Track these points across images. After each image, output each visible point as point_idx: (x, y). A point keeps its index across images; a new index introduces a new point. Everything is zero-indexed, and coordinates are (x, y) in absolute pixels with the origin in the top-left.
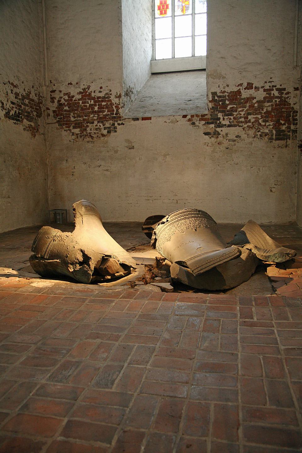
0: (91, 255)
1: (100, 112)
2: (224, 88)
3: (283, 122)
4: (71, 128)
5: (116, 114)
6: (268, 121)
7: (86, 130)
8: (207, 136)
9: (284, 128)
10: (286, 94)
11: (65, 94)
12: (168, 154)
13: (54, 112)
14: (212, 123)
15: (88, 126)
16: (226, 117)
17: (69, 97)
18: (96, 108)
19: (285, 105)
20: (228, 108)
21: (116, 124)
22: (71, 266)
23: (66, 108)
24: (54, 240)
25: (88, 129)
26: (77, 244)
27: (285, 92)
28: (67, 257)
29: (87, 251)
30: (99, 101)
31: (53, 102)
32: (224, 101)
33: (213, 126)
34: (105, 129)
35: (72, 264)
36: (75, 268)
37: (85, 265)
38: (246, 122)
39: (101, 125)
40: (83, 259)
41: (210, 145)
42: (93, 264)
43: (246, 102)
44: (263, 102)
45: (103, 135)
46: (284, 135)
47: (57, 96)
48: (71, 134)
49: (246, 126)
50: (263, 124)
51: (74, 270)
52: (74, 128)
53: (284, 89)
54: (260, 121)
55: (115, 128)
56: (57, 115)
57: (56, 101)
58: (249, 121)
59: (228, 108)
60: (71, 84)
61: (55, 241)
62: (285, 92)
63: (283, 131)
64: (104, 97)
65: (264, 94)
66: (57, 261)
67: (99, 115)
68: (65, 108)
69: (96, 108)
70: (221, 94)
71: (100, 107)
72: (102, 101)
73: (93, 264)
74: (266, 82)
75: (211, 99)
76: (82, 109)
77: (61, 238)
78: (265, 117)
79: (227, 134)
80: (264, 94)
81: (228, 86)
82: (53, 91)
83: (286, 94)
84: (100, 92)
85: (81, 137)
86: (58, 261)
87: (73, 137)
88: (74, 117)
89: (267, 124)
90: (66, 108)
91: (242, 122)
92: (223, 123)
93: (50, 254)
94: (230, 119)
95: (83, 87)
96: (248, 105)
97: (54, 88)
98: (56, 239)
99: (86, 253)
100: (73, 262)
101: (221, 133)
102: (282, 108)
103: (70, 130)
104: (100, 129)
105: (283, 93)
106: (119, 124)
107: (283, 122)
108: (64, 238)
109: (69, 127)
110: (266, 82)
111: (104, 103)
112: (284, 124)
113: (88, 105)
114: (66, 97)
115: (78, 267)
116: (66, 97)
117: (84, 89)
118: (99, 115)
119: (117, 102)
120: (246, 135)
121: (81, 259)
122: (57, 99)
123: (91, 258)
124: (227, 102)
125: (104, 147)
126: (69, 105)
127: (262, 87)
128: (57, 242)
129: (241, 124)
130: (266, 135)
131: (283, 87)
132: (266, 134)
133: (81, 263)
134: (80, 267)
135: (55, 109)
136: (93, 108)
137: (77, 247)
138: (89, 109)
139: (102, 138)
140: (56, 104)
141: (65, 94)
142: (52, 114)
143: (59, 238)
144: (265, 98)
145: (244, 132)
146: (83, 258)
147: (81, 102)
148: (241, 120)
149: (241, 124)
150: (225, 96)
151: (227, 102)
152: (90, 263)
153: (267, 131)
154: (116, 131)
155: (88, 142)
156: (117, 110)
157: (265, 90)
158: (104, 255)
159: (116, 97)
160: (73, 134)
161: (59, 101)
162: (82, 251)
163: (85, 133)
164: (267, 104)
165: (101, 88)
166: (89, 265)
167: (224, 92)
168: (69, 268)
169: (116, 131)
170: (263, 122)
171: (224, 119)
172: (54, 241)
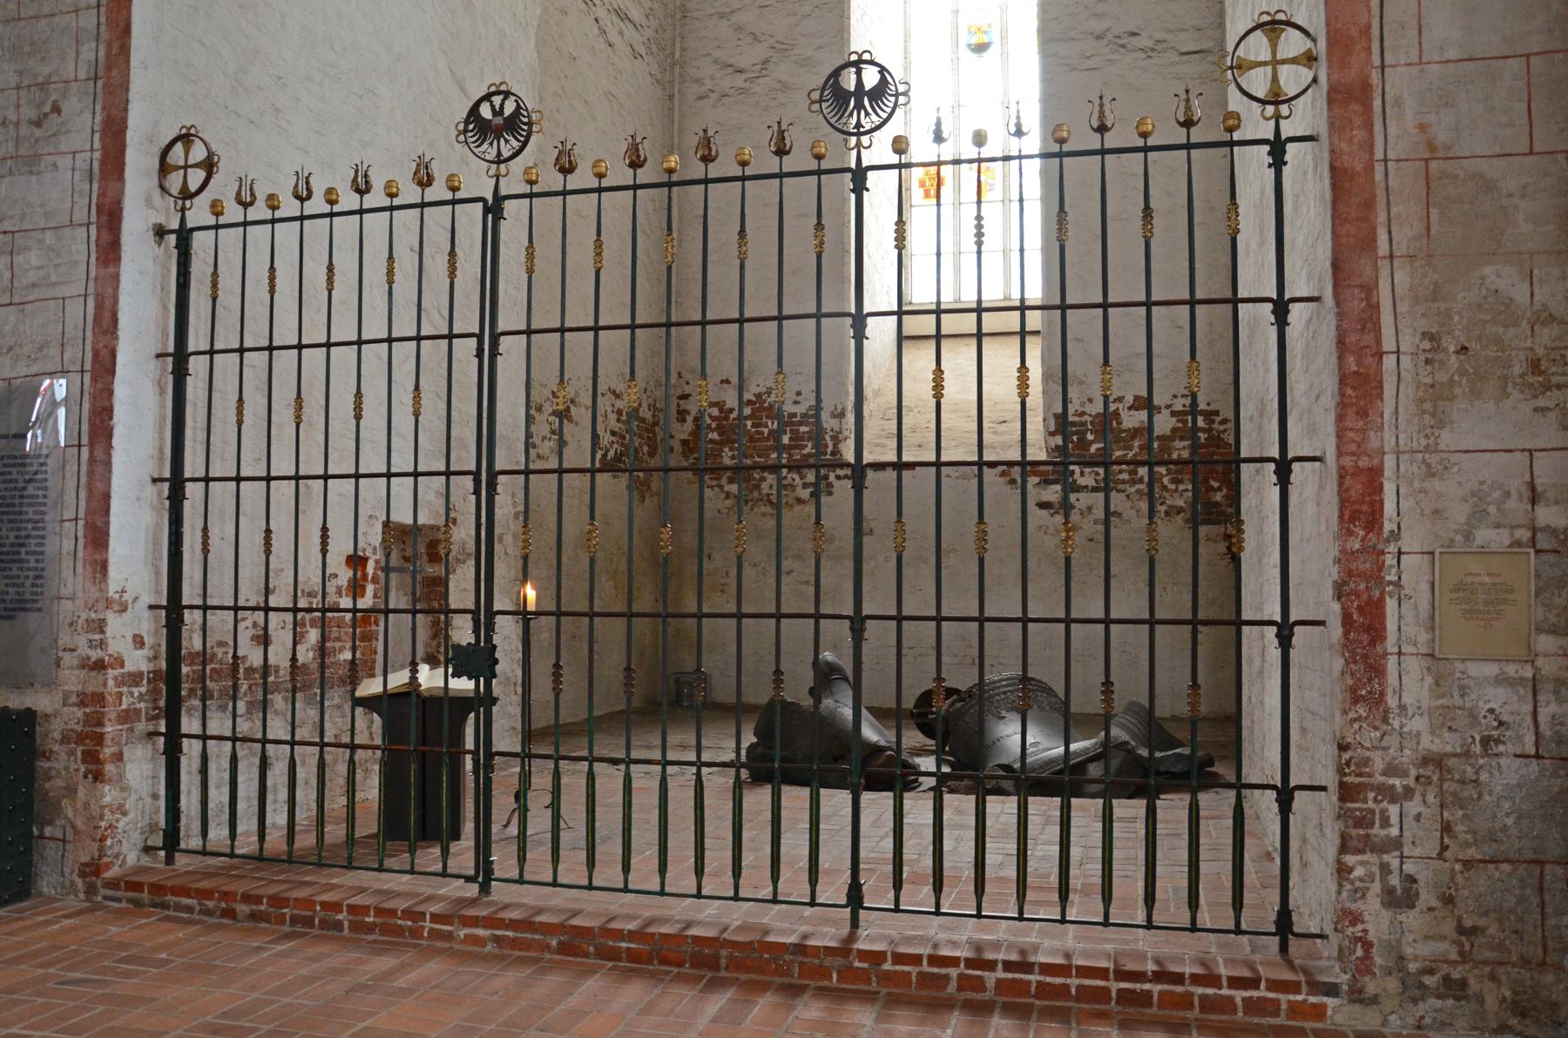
1: (795, 447)
2: (1083, 404)
3: (1216, 485)
4: (724, 481)
5: (833, 454)
6: (1181, 481)
7: (758, 487)
8: (1044, 512)
9: (1218, 497)
10: (1221, 423)
11: (712, 405)
12: (954, 550)
13: (684, 443)
14: (1055, 482)
15: (763, 479)
16: (1087, 470)
17: (721, 410)
18: (786, 440)
19: (1219, 447)
20: (1093, 449)
21: (832, 477)
23: (714, 436)
25: (765, 486)
27: (1218, 419)
30: (793, 424)
31: (683, 421)
32: (1082, 435)
33: (1058, 487)
34: (805, 486)
38: (1133, 482)
39: (796, 477)
41: (1051, 530)
43: (1133, 438)
44: (1171, 438)
45: (799, 501)
46: (1222, 513)
47: (692, 407)
48: (723, 496)
49: (1133, 490)
50: (1173, 487)
52: (731, 481)
53: (1217, 413)
54: (1166, 481)
55: (830, 485)
56: (692, 451)
57: (689, 419)
58: (1141, 480)
59: (1093, 449)
60: (727, 382)
62: (1218, 419)
63: (1217, 504)
64: (804, 415)
65: (1173, 422)
67: (791, 455)
68: (711, 436)
69: (786, 440)
70: (1076, 419)
71: (797, 437)
72: (801, 423)
74: (1175, 396)
75: (1052, 429)
76: (751, 440)
78: (1177, 472)
79: (1090, 509)
80: (1173, 422)
81: (1090, 400)
82: (685, 397)
83: (1221, 423)
84: (796, 402)
85: (746, 502)
87: (728, 503)
88: (733, 458)
89: (1181, 487)
90: (714, 436)
91: (1123, 482)
92: (1082, 481)
94: (1097, 474)
95: (758, 390)
96: (1136, 444)
97: (688, 390)
101: (1076, 504)
102: (1214, 453)
103: (721, 487)
104: (793, 487)
105: (1213, 422)
106: (838, 477)
107: (1216, 485)
109: (718, 479)
110: (1175, 396)
111: (803, 429)
112: (1219, 489)
113: (766, 431)
114: (715, 412)
116: (715, 412)
117: (758, 396)
118: (791, 455)
119: (836, 428)
120: (1133, 512)
122: (694, 413)
124: (1090, 437)
125: (801, 528)
126: (720, 429)
127: (1168, 407)
129: (1121, 487)
130: (1178, 513)
131: (1213, 407)
132: (1179, 511)
135: (685, 437)
136: (778, 439)
138: (768, 439)
139: (798, 508)
140: (689, 425)
141: (712, 405)
142: (678, 447)
144: (1174, 430)
145: (1128, 504)
147: (749, 423)
148: (1121, 477)
149: (1121, 487)
150: (1085, 424)
151: (1090, 437)
153: (1181, 503)
154: (830, 494)
155: (764, 515)
156: (835, 446)
157: (1173, 414)
159: (834, 415)
160: (728, 495)
161: (696, 419)
163: (756, 494)
164: (1178, 444)
165: (799, 394)
167: (1083, 414)
169: (830, 494)
170: (1173, 481)
171: (1082, 474)
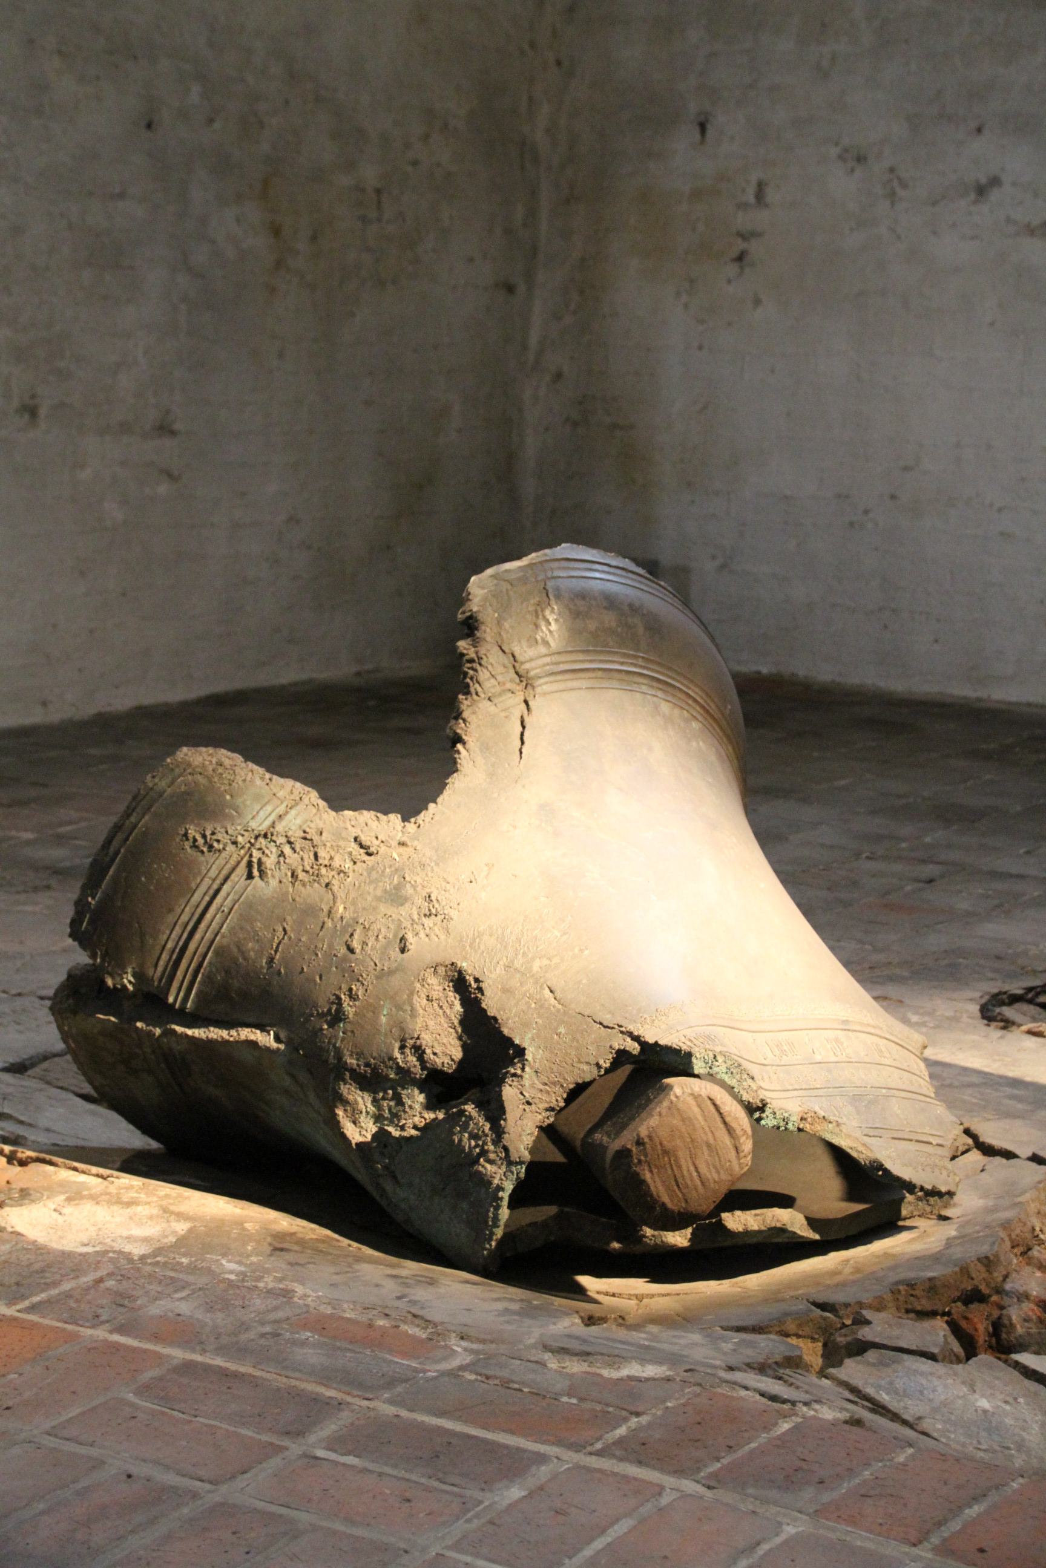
0: (526, 1025)
22: (363, 1101)
24: (250, 865)
26: (425, 921)
28: (337, 1017)
29: (506, 990)
35: (372, 1081)
36: (395, 1117)
37: (470, 1108)
40: (458, 1054)
42: (527, 1106)
51: (381, 1136)
61: (262, 873)
66: (254, 1044)
73: (527, 1106)
77: (309, 858)
86: (266, 1039)
93: (209, 979)
98: (270, 862)
99: (491, 1003)
100: (375, 1070)
108: (336, 863)
115: (417, 1112)
121: (445, 1047)
123: (520, 1052)
128: (273, 883)
133: (442, 1087)
134: (430, 1116)
137: (428, 944)
143: (292, 858)
146: (464, 1047)
152: (509, 1093)
158: (636, 1038)
162: (460, 983)
166: (495, 1112)
168: (340, 1112)
172: (250, 876)
